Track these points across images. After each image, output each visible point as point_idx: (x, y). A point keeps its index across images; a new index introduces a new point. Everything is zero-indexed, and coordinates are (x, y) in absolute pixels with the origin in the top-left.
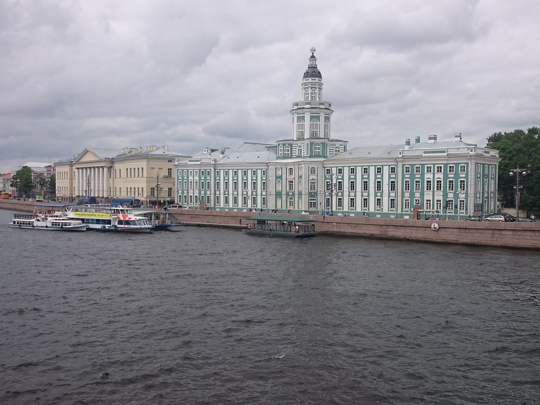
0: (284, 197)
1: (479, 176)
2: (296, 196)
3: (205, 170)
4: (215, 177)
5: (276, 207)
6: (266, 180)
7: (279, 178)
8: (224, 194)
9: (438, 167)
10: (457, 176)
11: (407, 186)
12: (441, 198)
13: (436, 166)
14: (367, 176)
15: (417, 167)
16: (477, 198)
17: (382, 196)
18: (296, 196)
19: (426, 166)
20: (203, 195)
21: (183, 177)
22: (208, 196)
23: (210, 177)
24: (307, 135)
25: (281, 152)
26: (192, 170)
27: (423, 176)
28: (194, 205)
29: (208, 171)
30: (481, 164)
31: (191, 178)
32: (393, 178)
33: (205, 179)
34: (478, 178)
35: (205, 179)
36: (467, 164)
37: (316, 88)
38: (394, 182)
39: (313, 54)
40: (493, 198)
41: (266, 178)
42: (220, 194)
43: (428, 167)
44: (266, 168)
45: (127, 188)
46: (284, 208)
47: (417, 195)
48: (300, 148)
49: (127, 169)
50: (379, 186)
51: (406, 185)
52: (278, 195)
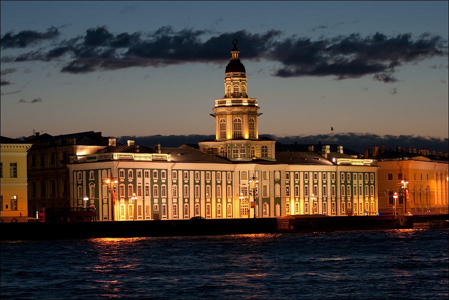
2: (272, 201)
3: (159, 170)
6: (231, 184)
8: (184, 202)
13: (359, 174)
18: (272, 201)
20: (157, 204)
21: (126, 180)
23: (167, 180)
26: (142, 170)
27: (352, 181)
28: (144, 218)
31: (139, 180)
33: (159, 182)
35: (159, 182)
36: (374, 173)
41: (232, 182)
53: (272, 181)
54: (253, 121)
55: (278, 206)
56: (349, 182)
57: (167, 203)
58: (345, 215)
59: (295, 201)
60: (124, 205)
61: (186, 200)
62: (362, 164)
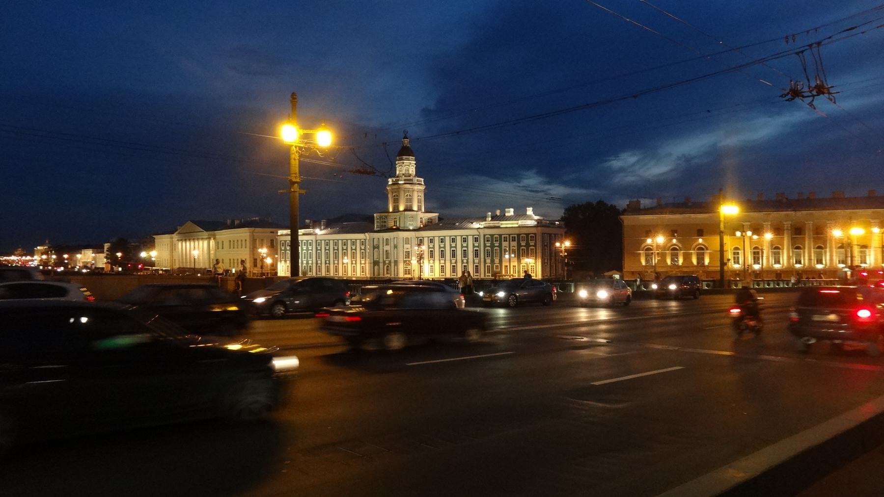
0: (381, 265)
1: (546, 244)
2: (393, 264)
3: (307, 241)
4: (317, 248)
5: (374, 275)
7: (376, 247)
8: (326, 263)
9: (513, 237)
10: (528, 245)
11: (488, 254)
12: (516, 264)
13: (511, 236)
14: (454, 245)
15: (496, 238)
16: (545, 263)
17: (467, 262)
18: (393, 264)
19: (503, 236)
21: (285, 248)
22: (310, 266)
24: (402, 208)
25: (378, 224)
29: (310, 243)
30: (547, 234)
32: (476, 247)
34: (545, 246)
36: (535, 234)
37: (409, 166)
38: (477, 250)
39: (405, 135)
40: (561, 262)
41: (365, 247)
42: (321, 264)
43: (504, 237)
44: (365, 238)
45: (230, 260)
46: (381, 276)
47: (497, 261)
48: (395, 220)
49: (230, 241)
50: (465, 254)
51: (487, 252)
52: (376, 263)
53: (392, 245)
54: (397, 196)
55: (396, 267)
56: (497, 244)
57: (312, 264)
58: (491, 277)
59: (429, 263)
60: (284, 265)
61: (327, 262)
62: (517, 226)
